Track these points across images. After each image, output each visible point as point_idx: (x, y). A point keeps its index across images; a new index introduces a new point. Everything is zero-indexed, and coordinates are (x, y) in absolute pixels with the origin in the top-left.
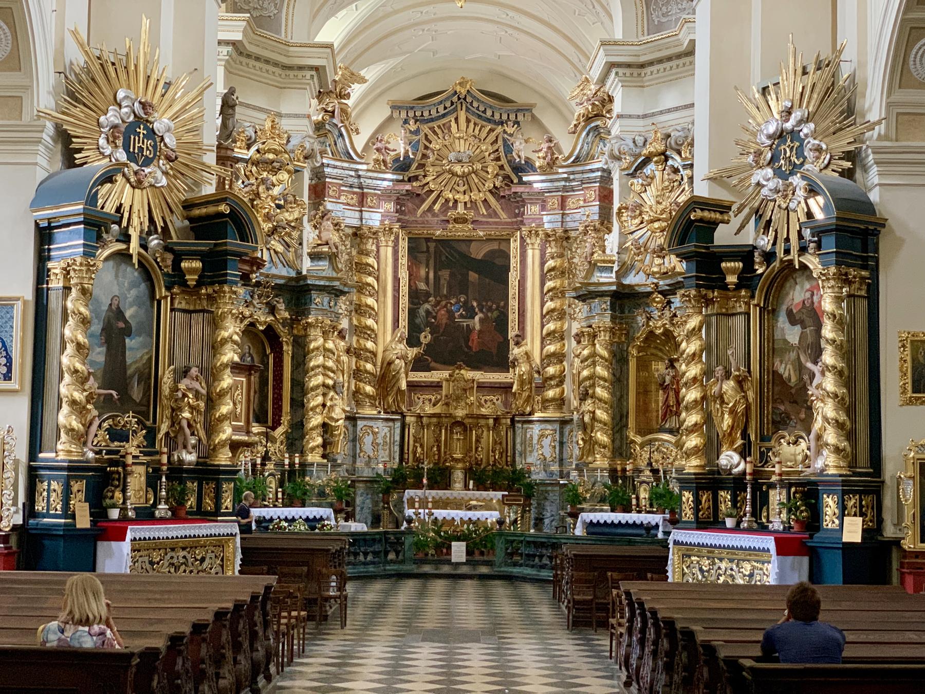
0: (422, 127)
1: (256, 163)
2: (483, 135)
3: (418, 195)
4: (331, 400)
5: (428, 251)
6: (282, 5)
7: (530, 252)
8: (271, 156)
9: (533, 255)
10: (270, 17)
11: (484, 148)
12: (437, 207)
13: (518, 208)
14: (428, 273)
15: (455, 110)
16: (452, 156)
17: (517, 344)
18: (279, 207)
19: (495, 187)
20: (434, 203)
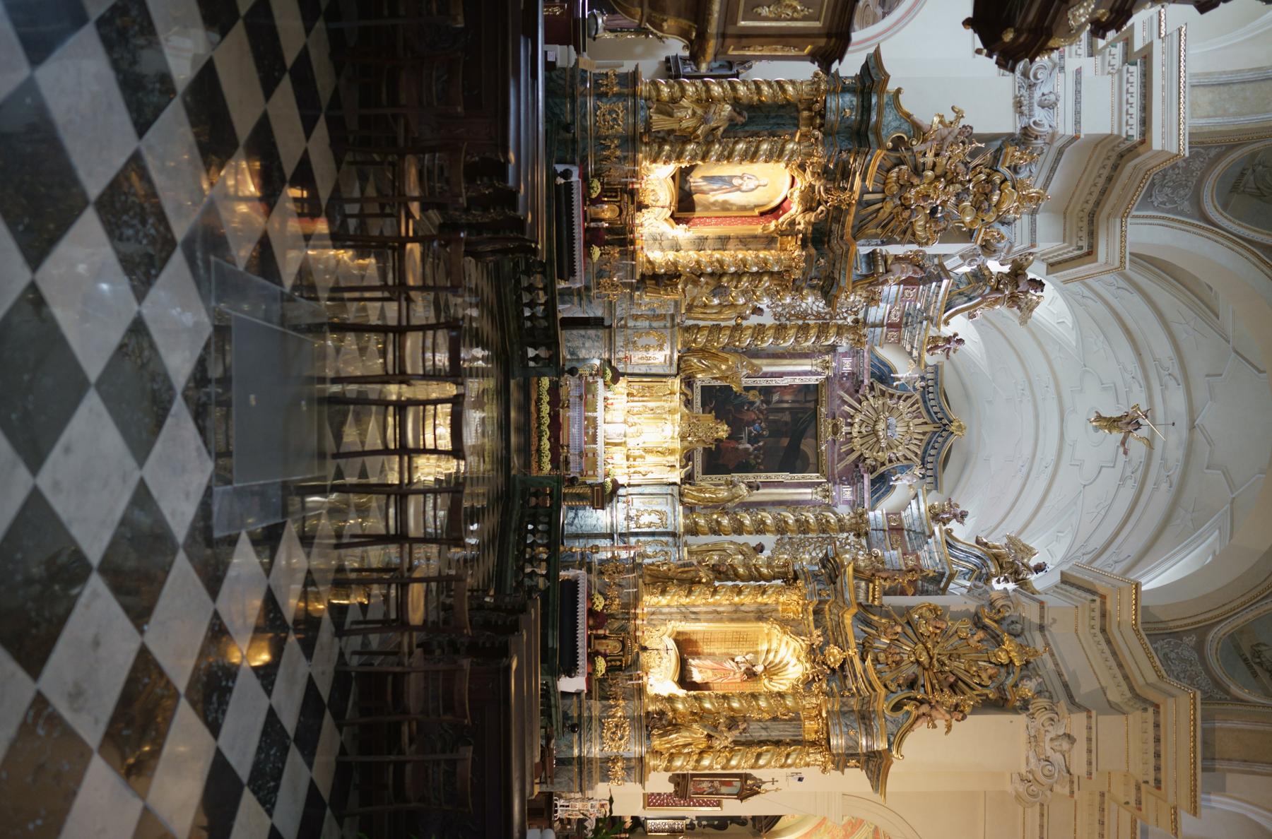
0: (918, 392)
1: (989, 181)
2: (912, 447)
3: (857, 391)
4: (707, 283)
5: (806, 402)
6: (1163, 211)
7: (809, 490)
8: (995, 198)
9: (807, 494)
10: (1151, 196)
11: (900, 448)
12: (846, 408)
13: (847, 480)
14: (787, 402)
15: (934, 422)
16: (892, 420)
17: (751, 486)
18: (934, 211)
19: (865, 459)
20: (850, 406)
